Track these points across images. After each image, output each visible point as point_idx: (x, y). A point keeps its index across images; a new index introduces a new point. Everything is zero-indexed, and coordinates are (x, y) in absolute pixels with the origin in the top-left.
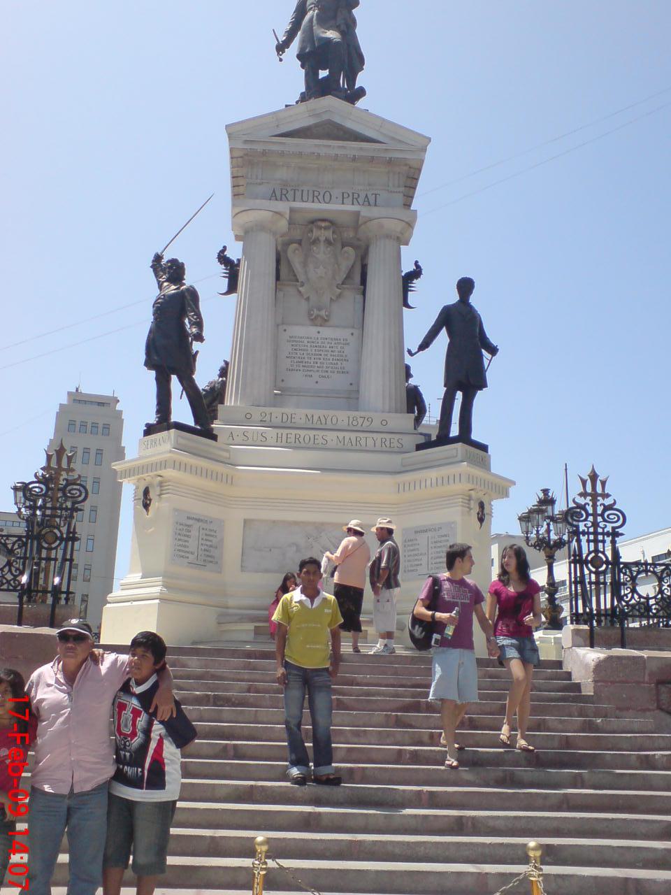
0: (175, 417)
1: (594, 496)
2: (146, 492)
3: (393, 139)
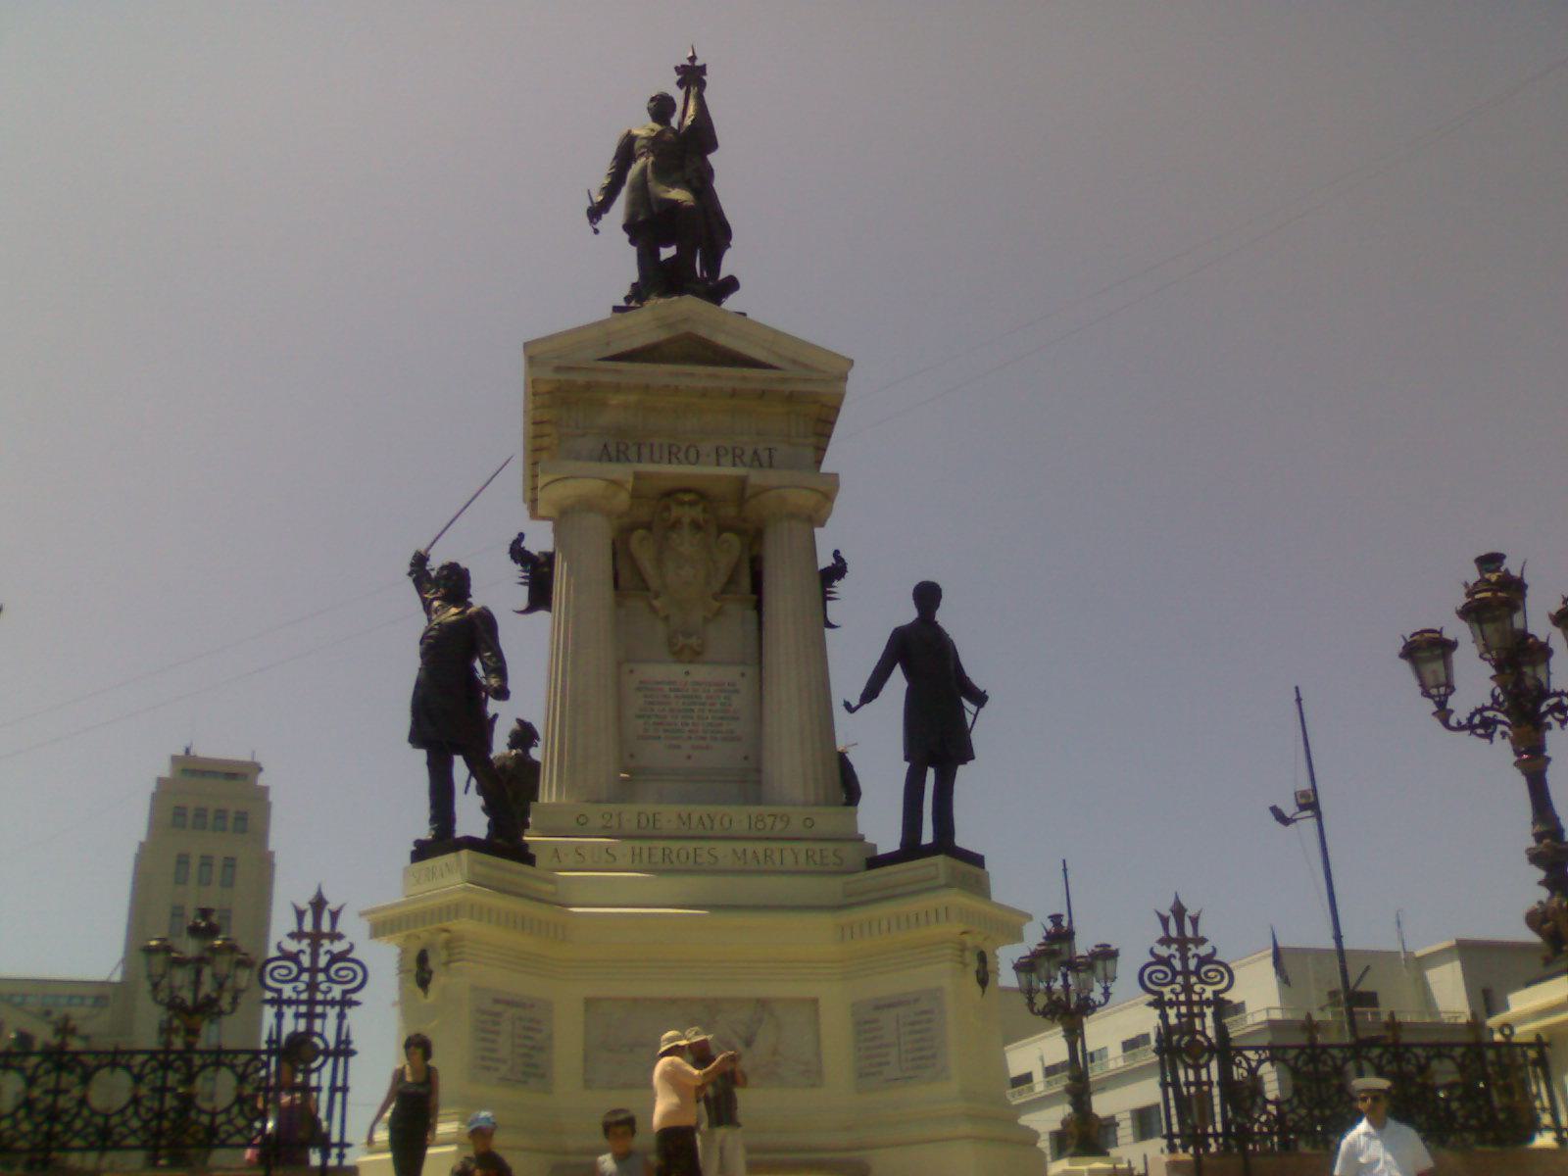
0: (461, 830)
1: (1182, 942)
3: (795, 362)
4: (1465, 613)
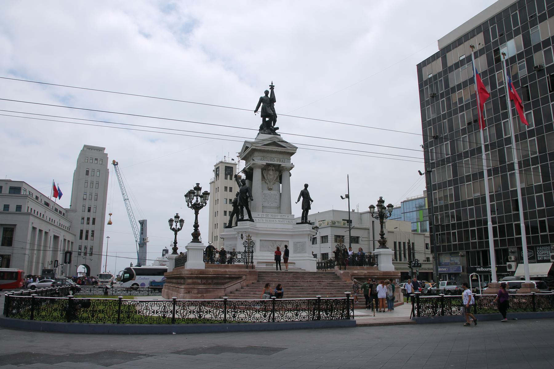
2: (242, 235)
4: (377, 206)
